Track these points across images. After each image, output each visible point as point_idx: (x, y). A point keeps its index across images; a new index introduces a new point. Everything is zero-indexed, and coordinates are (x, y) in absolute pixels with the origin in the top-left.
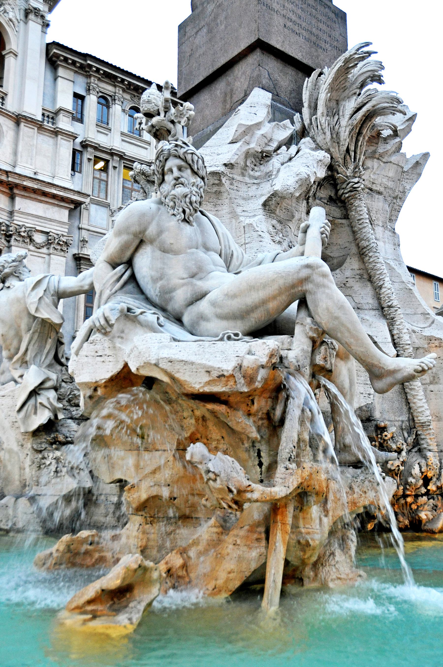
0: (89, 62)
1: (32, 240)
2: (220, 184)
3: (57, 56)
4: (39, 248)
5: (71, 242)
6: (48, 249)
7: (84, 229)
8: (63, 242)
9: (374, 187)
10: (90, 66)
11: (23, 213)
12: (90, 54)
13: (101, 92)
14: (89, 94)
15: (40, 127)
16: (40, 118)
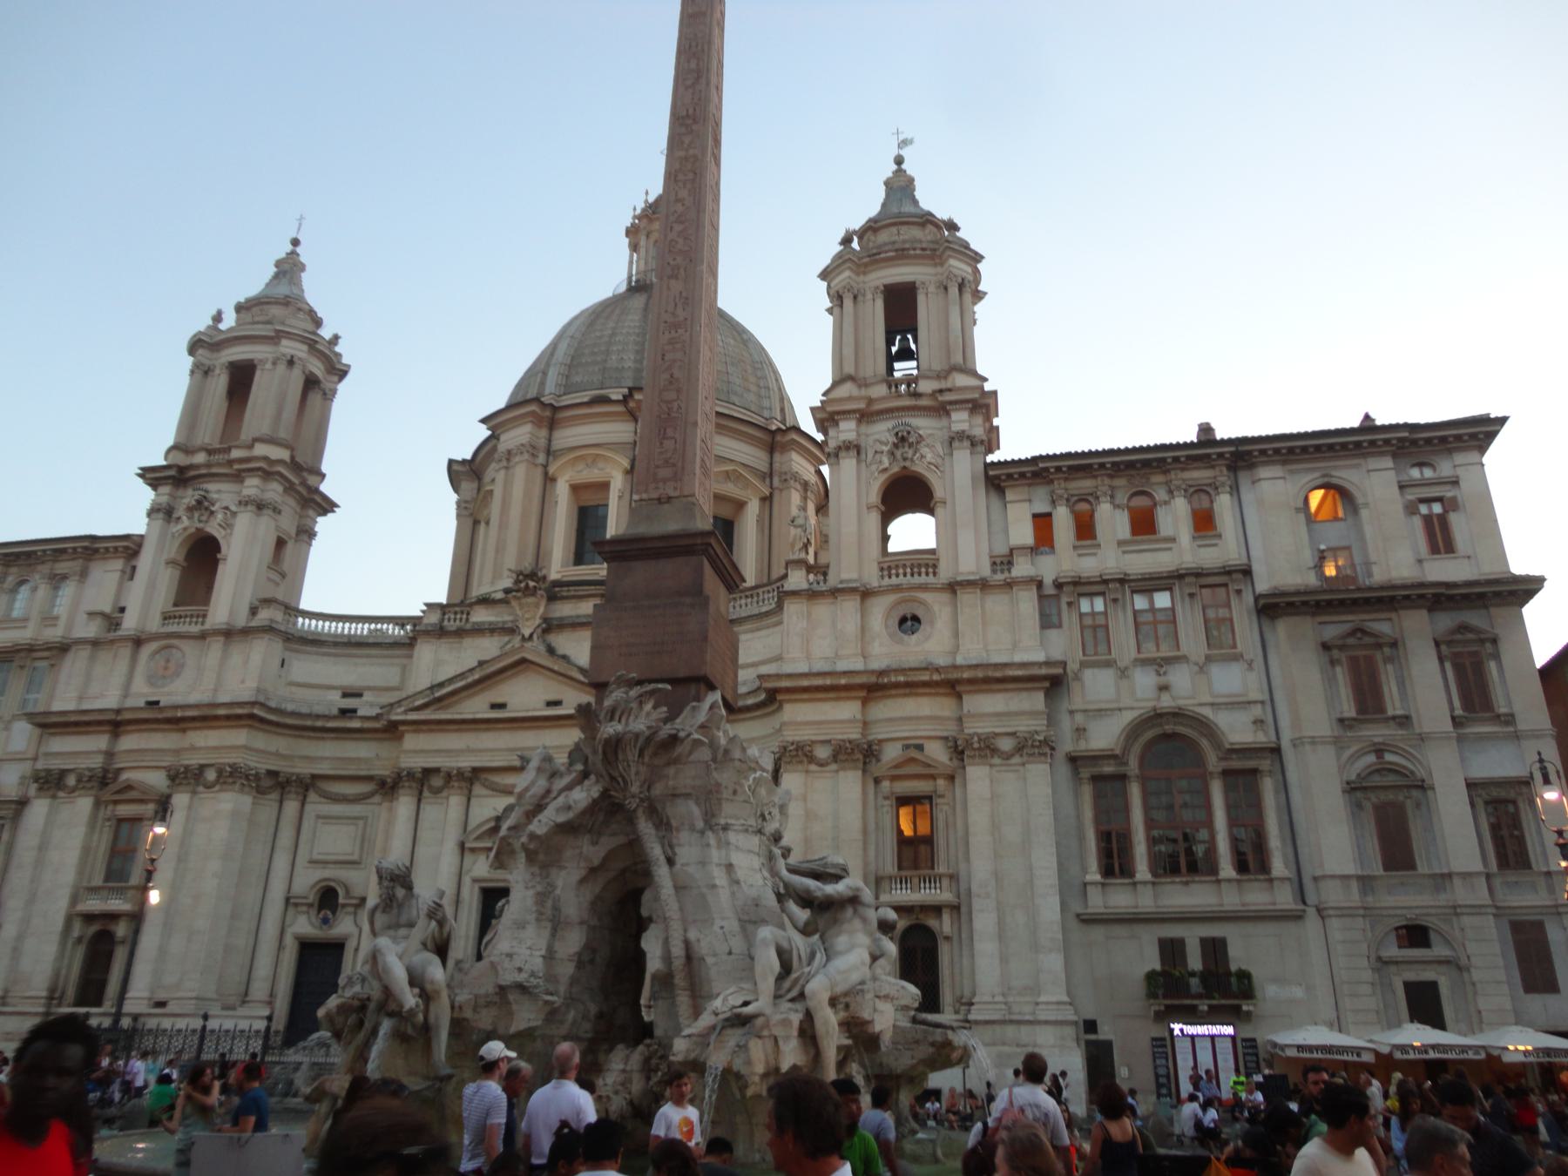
0: (1041, 465)
1: (994, 751)
2: (509, 844)
3: (998, 477)
4: (1007, 759)
5: (1053, 738)
6: (1021, 756)
7: (1077, 711)
8: (1040, 741)
9: (678, 792)
10: (1046, 469)
11: (973, 716)
12: (1037, 454)
13: (1072, 495)
14: (1055, 507)
15: (983, 585)
16: (986, 571)
